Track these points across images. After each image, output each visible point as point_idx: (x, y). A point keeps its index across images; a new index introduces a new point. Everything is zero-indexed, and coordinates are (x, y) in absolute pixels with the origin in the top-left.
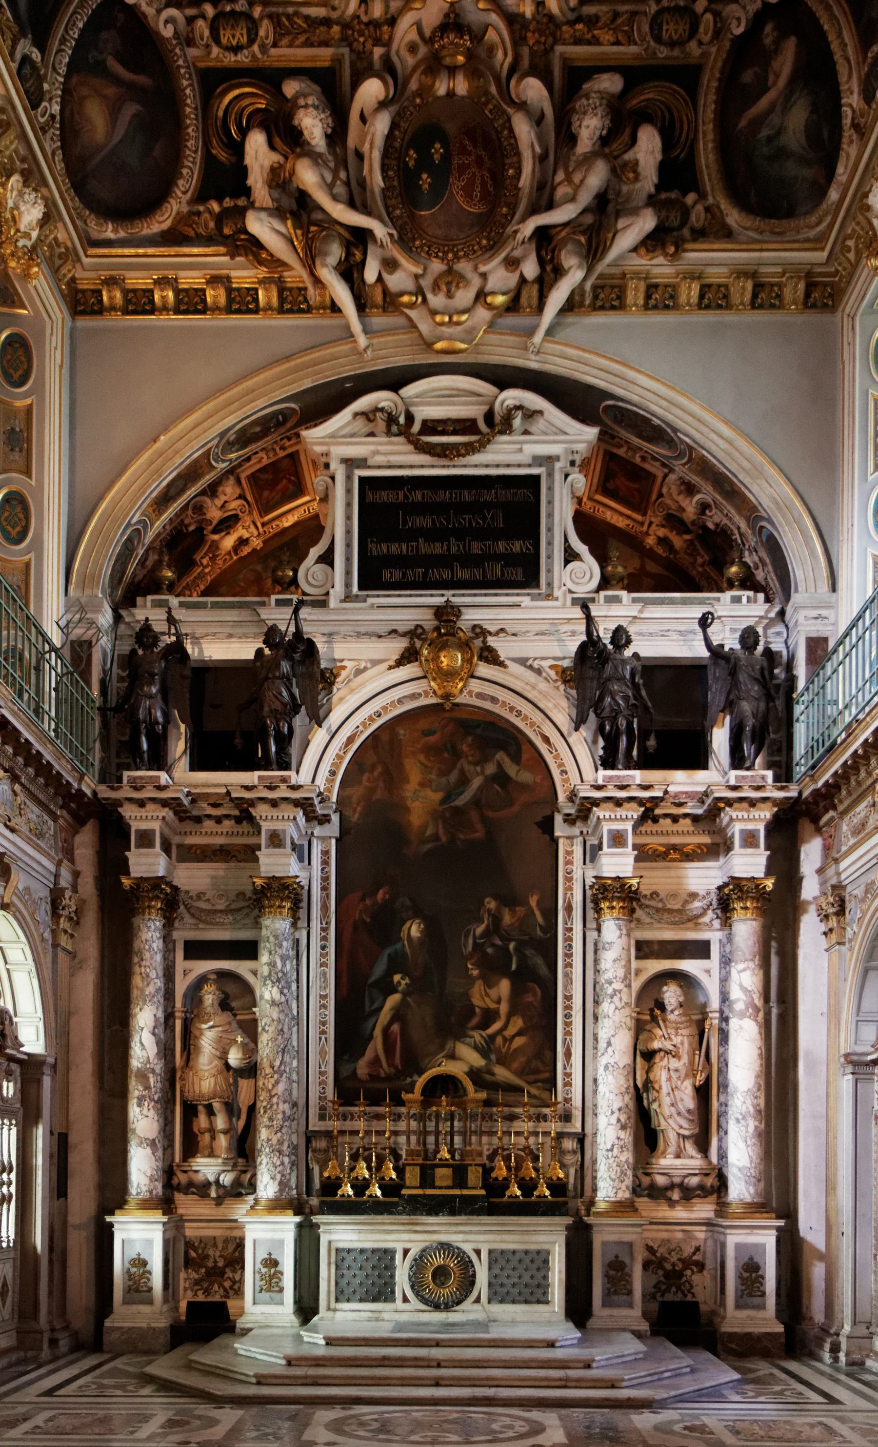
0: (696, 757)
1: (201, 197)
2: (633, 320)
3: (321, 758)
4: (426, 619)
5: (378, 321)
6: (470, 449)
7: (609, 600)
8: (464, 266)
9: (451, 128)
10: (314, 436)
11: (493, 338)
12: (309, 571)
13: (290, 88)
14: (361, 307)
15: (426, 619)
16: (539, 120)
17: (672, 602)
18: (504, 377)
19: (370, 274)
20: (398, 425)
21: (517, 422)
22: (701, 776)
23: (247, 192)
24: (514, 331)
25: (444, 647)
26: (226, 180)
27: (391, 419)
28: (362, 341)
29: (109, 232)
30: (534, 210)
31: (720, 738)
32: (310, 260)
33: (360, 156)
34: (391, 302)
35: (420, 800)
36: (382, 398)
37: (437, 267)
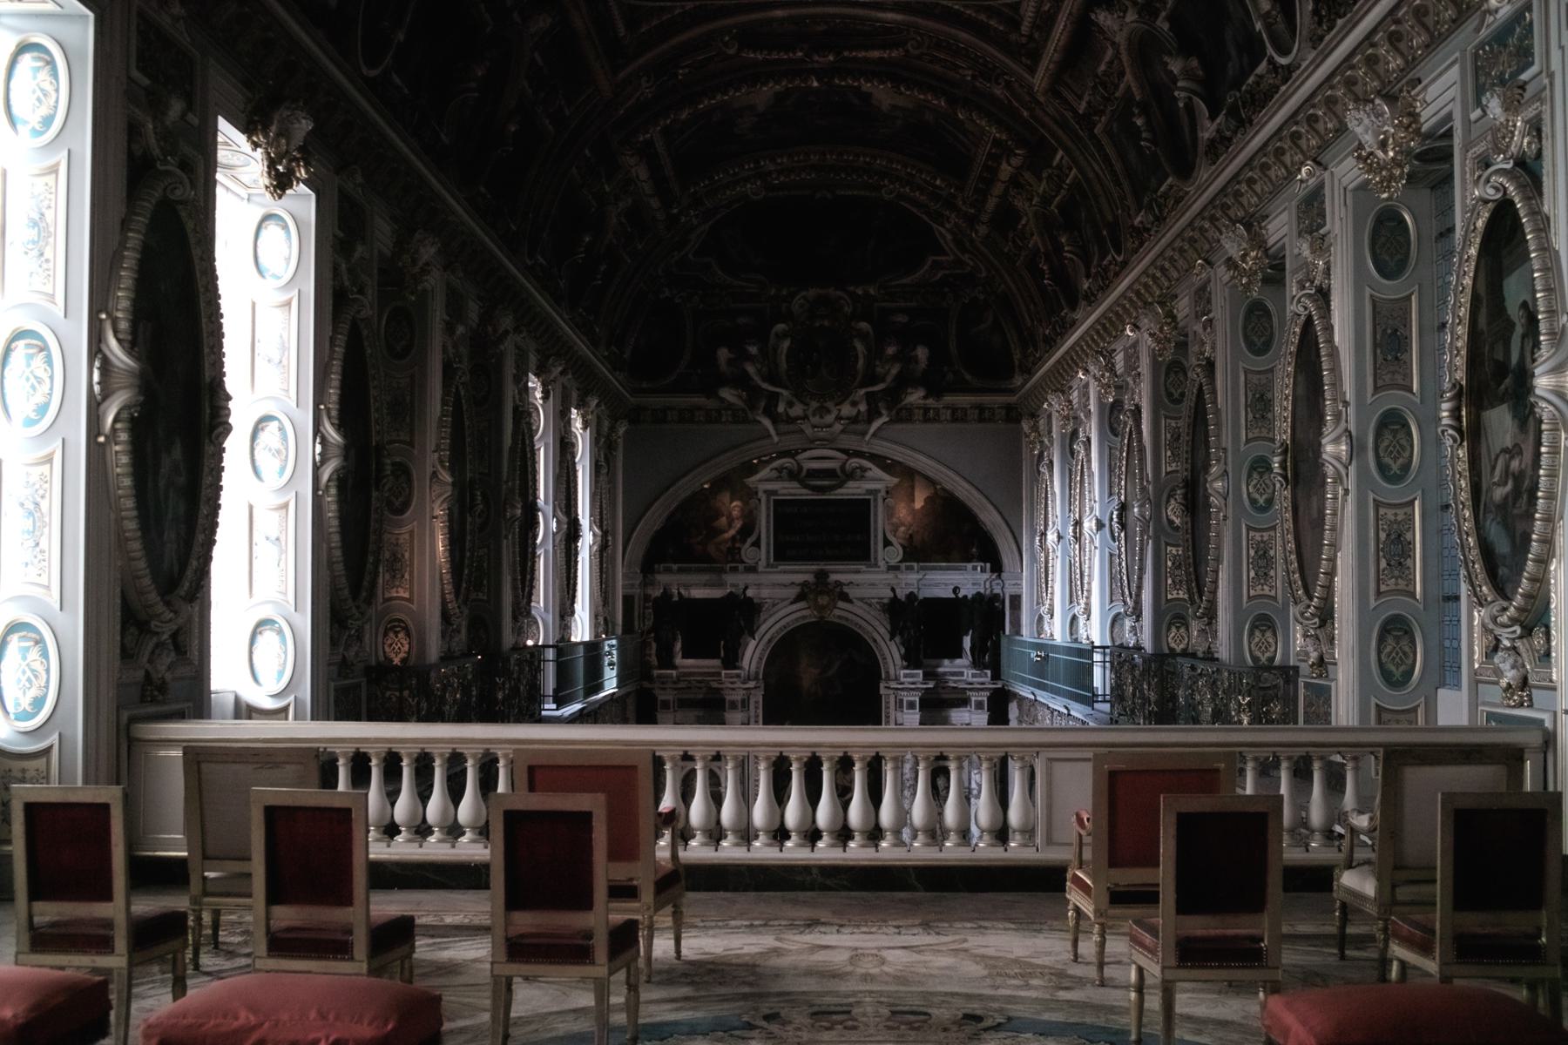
0: (958, 653)
3: (753, 654)
4: (810, 578)
5: (783, 427)
7: (908, 568)
8: (829, 404)
10: (752, 481)
12: (747, 552)
13: (742, 320)
14: (774, 422)
15: (810, 578)
16: (863, 336)
17: (941, 569)
19: (781, 408)
20: (793, 475)
22: (958, 661)
24: (855, 433)
25: (821, 593)
30: (862, 386)
31: (967, 642)
32: (753, 408)
34: (791, 420)
35: (808, 675)
36: (786, 462)
37: (814, 404)
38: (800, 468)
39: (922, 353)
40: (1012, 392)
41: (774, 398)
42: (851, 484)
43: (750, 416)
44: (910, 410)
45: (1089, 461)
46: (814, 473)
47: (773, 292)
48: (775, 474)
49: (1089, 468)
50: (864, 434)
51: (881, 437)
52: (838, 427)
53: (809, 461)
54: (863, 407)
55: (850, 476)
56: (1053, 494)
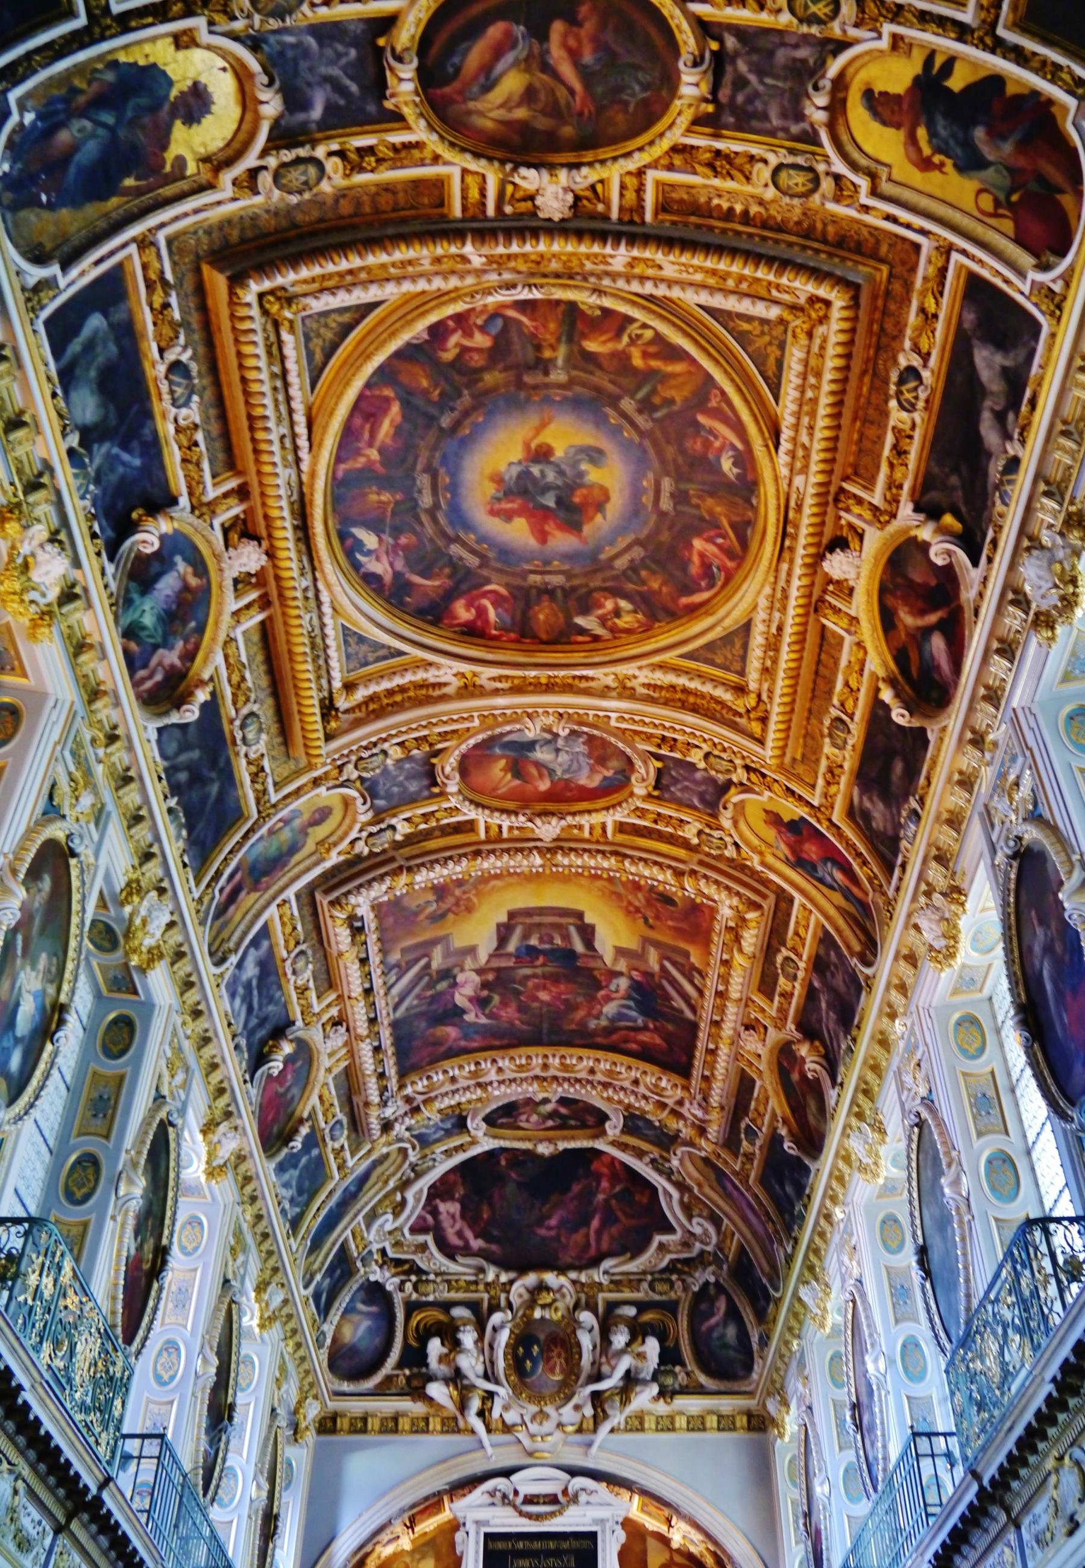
1: (400, 1365)
2: (649, 1436)
6: (552, 1514)
8: (549, 1409)
9: (542, 1337)
11: (567, 1449)
18: (574, 1472)
19: (496, 1413)
21: (583, 1497)
23: (427, 1365)
24: (579, 1444)
26: (415, 1357)
27: (505, 1496)
28: (490, 1450)
29: (346, 1387)
33: (491, 1347)
34: (507, 1429)
36: (499, 1483)
37: (534, 1408)
38: (516, 1493)
39: (652, 1347)
40: (750, 1394)
41: (490, 1395)
42: (572, 1511)
43: (461, 1424)
44: (640, 1417)
45: (863, 1295)
46: (530, 1500)
47: (490, 1277)
48: (487, 1499)
49: (865, 1301)
50: (590, 1445)
51: (606, 1450)
52: (558, 1435)
53: (526, 1483)
54: (589, 1411)
55: (575, 1499)
56: (817, 1436)
